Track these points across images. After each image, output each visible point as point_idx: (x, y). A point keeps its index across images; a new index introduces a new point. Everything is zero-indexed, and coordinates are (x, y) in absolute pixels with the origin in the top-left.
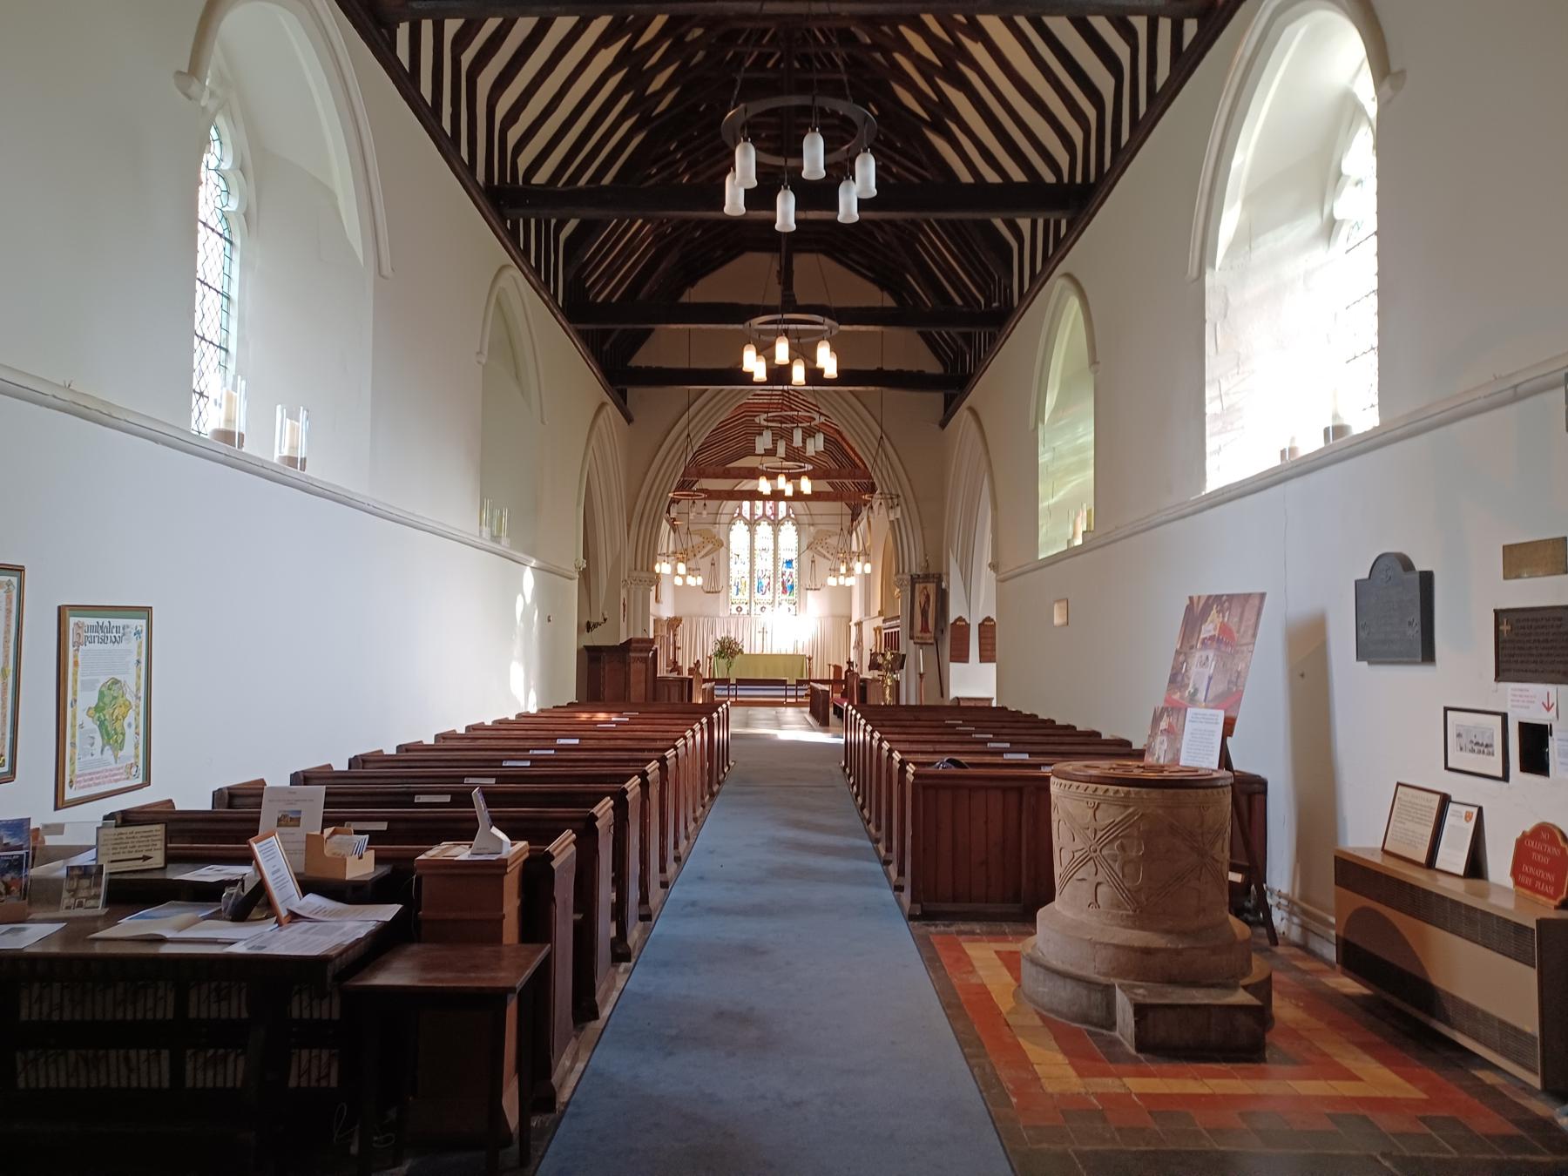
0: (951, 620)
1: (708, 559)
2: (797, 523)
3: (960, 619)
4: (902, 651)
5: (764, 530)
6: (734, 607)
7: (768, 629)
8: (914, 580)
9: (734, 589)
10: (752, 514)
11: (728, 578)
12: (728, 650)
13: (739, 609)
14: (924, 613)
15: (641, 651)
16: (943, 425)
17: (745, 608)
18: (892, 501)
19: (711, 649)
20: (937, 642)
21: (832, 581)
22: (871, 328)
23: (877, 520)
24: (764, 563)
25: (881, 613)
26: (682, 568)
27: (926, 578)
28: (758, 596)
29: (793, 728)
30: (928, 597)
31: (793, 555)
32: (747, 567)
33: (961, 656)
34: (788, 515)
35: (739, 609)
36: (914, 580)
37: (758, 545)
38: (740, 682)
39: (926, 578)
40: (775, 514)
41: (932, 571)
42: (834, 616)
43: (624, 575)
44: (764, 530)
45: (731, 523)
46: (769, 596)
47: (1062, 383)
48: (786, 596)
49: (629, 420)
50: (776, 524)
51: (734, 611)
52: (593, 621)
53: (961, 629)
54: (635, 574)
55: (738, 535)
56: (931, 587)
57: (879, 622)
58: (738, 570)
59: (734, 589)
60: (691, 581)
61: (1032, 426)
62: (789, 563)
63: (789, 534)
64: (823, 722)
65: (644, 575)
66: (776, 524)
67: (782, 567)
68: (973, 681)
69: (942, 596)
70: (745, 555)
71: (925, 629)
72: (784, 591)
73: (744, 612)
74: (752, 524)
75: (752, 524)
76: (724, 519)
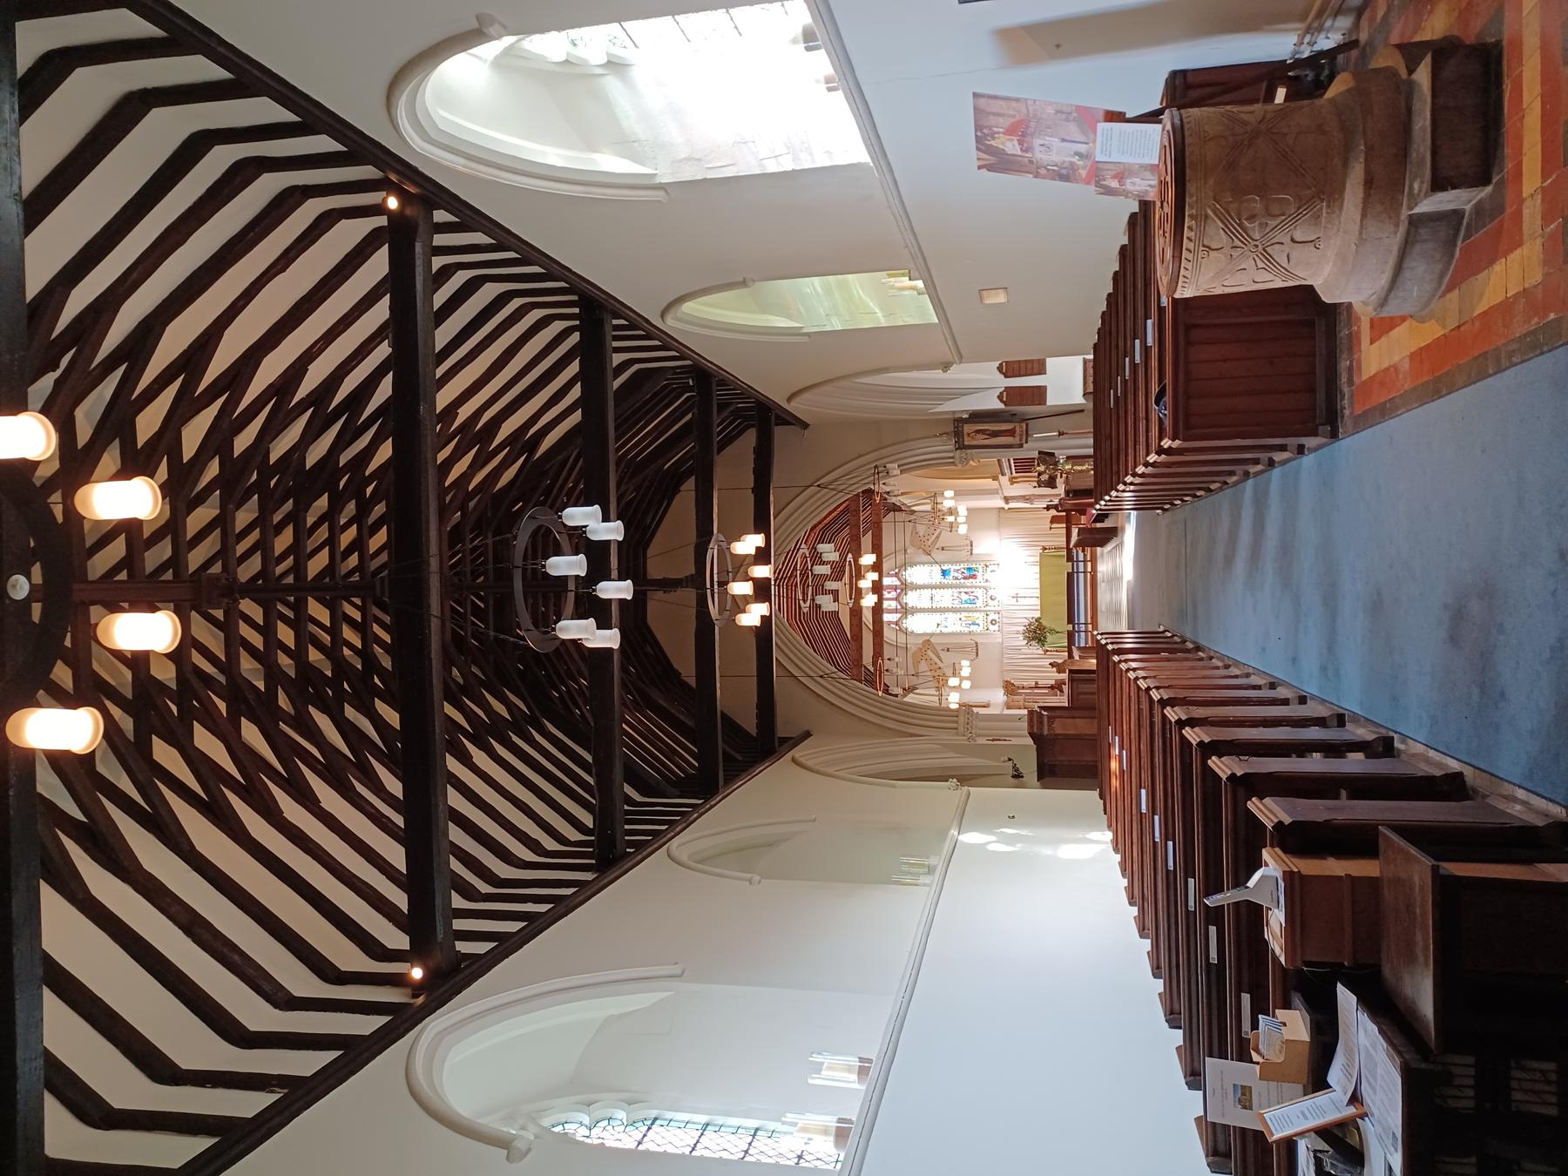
0: (1002, 406)
1: (942, 654)
2: (905, 566)
3: (1000, 397)
4: (1035, 454)
5: (912, 599)
6: (992, 628)
8: (961, 446)
9: (973, 628)
10: (896, 611)
11: (961, 634)
12: (1037, 633)
13: (993, 622)
14: (995, 434)
15: (1041, 723)
16: (805, 426)
17: (992, 616)
18: (880, 472)
19: (1036, 650)
20: (1024, 419)
21: (963, 530)
22: (715, 501)
23: (900, 486)
24: (945, 598)
25: (995, 478)
26: (953, 682)
27: (958, 434)
28: (979, 603)
29: (1120, 563)
30: (978, 432)
31: (937, 569)
32: (951, 616)
33: (1039, 394)
34: (896, 575)
35: (993, 622)
36: (961, 446)
37: (927, 605)
38: (1071, 620)
39: (958, 434)
41: (951, 429)
43: (962, 740)
44: (912, 599)
45: (906, 632)
46: (979, 593)
47: (765, 312)
48: (979, 575)
49: (807, 735)
50: (905, 587)
51: (996, 627)
52: (1011, 772)
53: (1010, 395)
54: (961, 729)
55: (918, 624)
56: (968, 428)
57: (1004, 480)
58: (953, 624)
59: (973, 628)
60: (966, 672)
61: (806, 339)
62: (944, 573)
63: (916, 574)
64: (1113, 533)
65: (961, 719)
66: (905, 587)
67: (949, 580)
68: (1066, 380)
69: (977, 416)
70: (937, 617)
71: (1011, 433)
72: (974, 577)
73: (996, 617)
74: (906, 611)
75: (906, 611)
76: (902, 639)
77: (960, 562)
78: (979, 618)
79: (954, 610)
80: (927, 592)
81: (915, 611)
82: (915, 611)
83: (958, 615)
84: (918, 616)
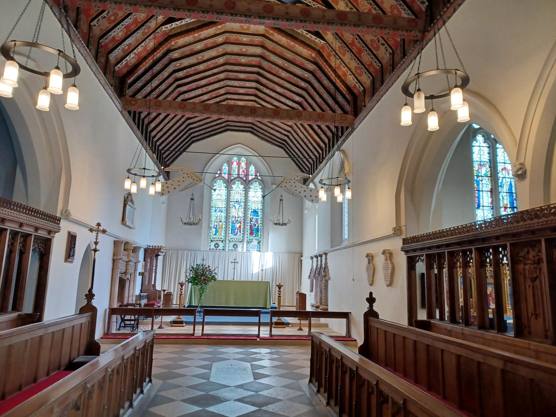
1: (189, 192)
5: (238, 187)
6: (213, 244)
7: (238, 260)
11: (210, 221)
12: (201, 277)
13: (217, 245)
17: (221, 245)
24: (237, 212)
25: (397, 231)
32: (223, 215)
35: (217, 245)
38: (209, 312)
40: (247, 175)
44: (238, 187)
45: (214, 179)
46: (239, 236)
48: (251, 237)
50: (247, 183)
51: (212, 247)
58: (217, 216)
62: (255, 212)
66: (247, 183)
72: (251, 234)
73: (221, 247)
74: (229, 183)
75: (229, 183)
76: (208, 178)
77: (263, 223)
78: (221, 235)
79: (227, 217)
81: (229, 188)
82: (229, 188)
83: (223, 220)
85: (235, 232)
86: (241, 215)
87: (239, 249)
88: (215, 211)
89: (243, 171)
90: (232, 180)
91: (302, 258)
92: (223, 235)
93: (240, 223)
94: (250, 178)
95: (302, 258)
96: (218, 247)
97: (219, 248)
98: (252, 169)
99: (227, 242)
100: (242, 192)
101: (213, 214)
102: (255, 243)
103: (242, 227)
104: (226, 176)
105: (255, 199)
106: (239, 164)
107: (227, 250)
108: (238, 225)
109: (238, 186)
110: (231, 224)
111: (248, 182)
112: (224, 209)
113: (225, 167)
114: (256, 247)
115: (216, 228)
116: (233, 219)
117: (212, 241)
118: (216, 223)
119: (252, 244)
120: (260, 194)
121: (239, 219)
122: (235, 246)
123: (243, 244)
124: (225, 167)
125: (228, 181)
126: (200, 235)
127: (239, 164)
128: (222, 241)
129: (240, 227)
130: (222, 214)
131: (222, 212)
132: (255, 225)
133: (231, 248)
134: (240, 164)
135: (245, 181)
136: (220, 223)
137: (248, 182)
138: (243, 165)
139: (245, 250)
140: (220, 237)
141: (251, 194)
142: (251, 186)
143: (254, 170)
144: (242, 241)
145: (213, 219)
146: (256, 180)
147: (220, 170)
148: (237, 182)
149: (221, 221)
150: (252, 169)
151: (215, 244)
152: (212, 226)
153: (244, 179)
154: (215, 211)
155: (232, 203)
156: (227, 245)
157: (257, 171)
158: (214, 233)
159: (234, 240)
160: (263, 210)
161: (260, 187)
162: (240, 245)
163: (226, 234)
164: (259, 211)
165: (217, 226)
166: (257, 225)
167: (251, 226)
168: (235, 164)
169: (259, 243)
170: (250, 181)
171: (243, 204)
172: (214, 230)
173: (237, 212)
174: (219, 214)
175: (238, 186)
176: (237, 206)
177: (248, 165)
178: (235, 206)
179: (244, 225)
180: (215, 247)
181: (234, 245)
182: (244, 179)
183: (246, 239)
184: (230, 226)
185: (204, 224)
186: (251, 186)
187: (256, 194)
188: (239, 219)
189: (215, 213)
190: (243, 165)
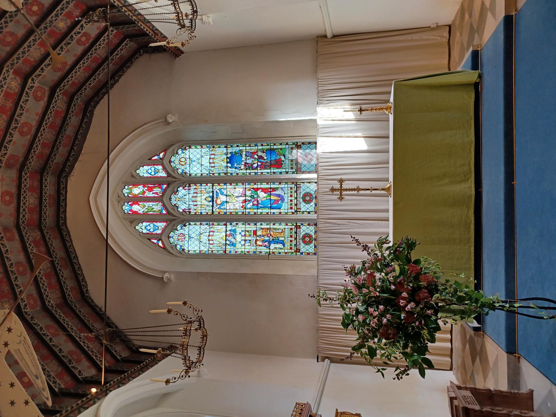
5: (184, 199)
6: (304, 248)
11: (254, 257)
17: (305, 229)
24: (234, 198)
28: (285, 207)
31: (221, 152)
32: (240, 227)
34: (160, 162)
42: (315, 71)
44: (184, 199)
45: (169, 250)
46: (285, 190)
50: (175, 181)
51: (310, 248)
55: (195, 239)
58: (242, 240)
62: (231, 159)
66: (175, 181)
72: (278, 164)
74: (175, 219)
75: (175, 219)
79: (246, 219)
80: (205, 191)
81: (187, 218)
82: (187, 218)
83: (252, 227)
84: (194, 229)
85: (276, 201)
86: (240, 189)
87: (313, 188)
88: (233, 245)
89: (150, 189)
90: (169, 213)
91: (329, 35)
92: (283, 226)
93: (257, 190)
94: (163, 174)
95: (329, 35)
96: (310, 236)
97: (312, 234)
98: (144, 171)
99: (299, 216)
100: (192, 191)
101: (240, 248)
102: (298, 154)
103: (265, 186)
104: (162, 225)
105: (205, 161)
106: (136, 200)
107: (314, 216)
108: (262, 195)
109: (180, 199)
110: (260, 211)
111: (170, 179)
112: (229, 227)
113: (144, 227)
114: (308, 151)
115: (270, 243)
116: (249, 205)
117: (298, 250)
118: (259, 243)
119: (300, 160)
120: (194, 153)
121: (248, 193)
122: (307, 198)
123: (303, 181)
124: (144, 227)
125: (172, 221)
126: (284, 276)
127: (136, 200)
128: (298, 227)
129: (264, 190)
130: (239, 230)
131: (234, 231)
132: (260, 157)
133: (311, 207)
134: (135, 196)
135: (168, 185)
136: (259, 233)
137: (170, 179)
138: (137, 191)
139: (314, 176)
140: (287, 232)
141: (195, 170)
142: (180, 171)
143: (146, 168)
144: (296, 183)
145: (249, 248)
146: (165, 162)
147: (149, 237)
148: (174, 202)
149: (255, 232)
150: (144, 171)
151: (305, 242)
152: (264, 250)
153: (165, 186)
154: (233, 245)
155: (216, 210)
156: (306, 216)
157: (150, 162)
158: (280, 246)
159: (294, 202)
160: (227, 142)
161: (180, 152)
162: (305, 188)
163: (280, 221)
164: (230, 150)
165: (264, 241)
166: (260, 154)
167: (263, 166)
168: (136, 208)
169: (298, 147)
170: (169, 175)
171: (217, 187)
172: (273, 246)
173: (234, 198)
174: (239, 238)
175: (180, 199)
176: (223, 198)
177: (136, 181)
178: (222, 203)
179: (261, 181)
180: (310, 242)
181: (305, 201)
182: (165, 186)
183: (290, 176)
184: (265, 211)
185: (261, 268)
186: (180, 171)
187: (196, 160)
188: (248, 193)
189: (238, 246)
190: (137, 191)
